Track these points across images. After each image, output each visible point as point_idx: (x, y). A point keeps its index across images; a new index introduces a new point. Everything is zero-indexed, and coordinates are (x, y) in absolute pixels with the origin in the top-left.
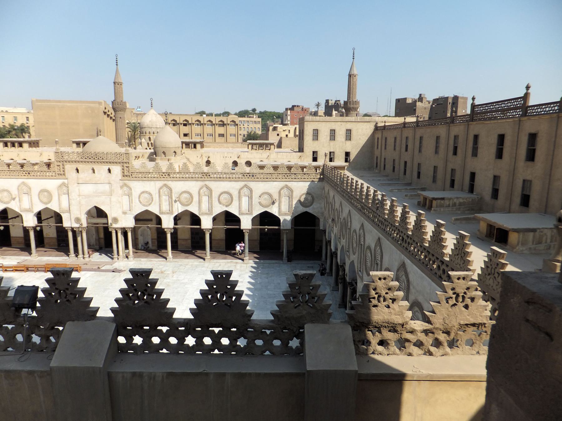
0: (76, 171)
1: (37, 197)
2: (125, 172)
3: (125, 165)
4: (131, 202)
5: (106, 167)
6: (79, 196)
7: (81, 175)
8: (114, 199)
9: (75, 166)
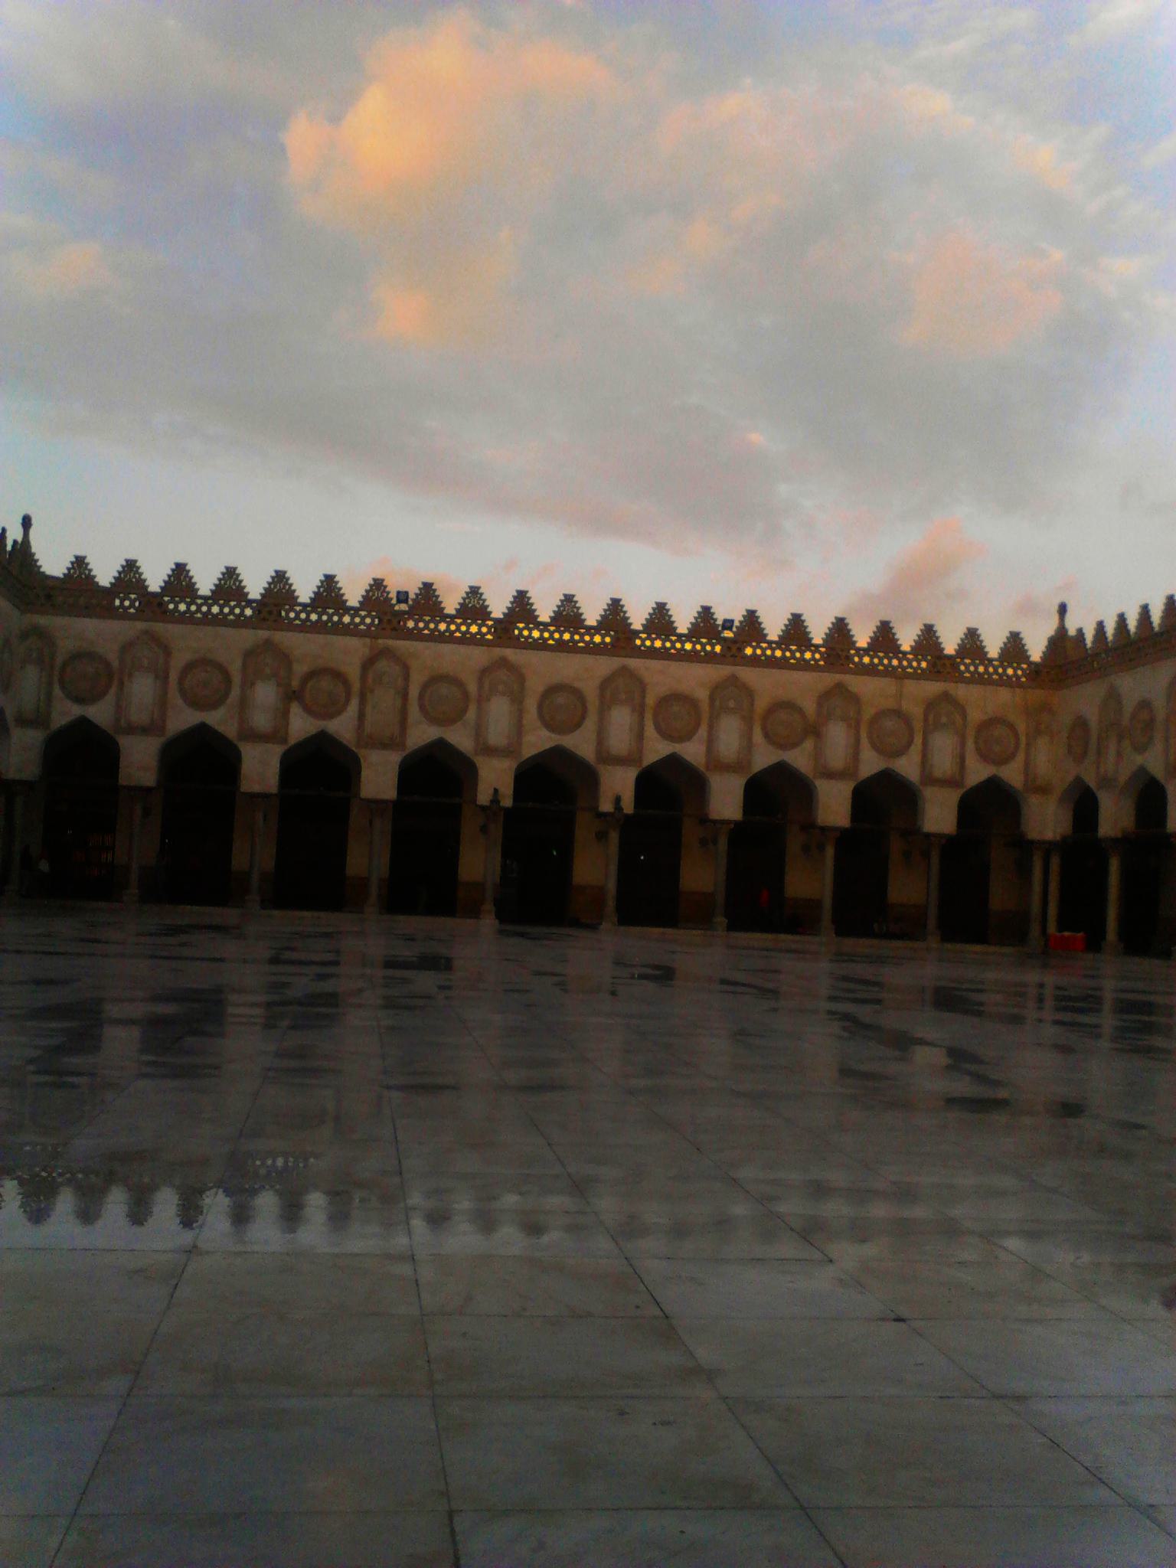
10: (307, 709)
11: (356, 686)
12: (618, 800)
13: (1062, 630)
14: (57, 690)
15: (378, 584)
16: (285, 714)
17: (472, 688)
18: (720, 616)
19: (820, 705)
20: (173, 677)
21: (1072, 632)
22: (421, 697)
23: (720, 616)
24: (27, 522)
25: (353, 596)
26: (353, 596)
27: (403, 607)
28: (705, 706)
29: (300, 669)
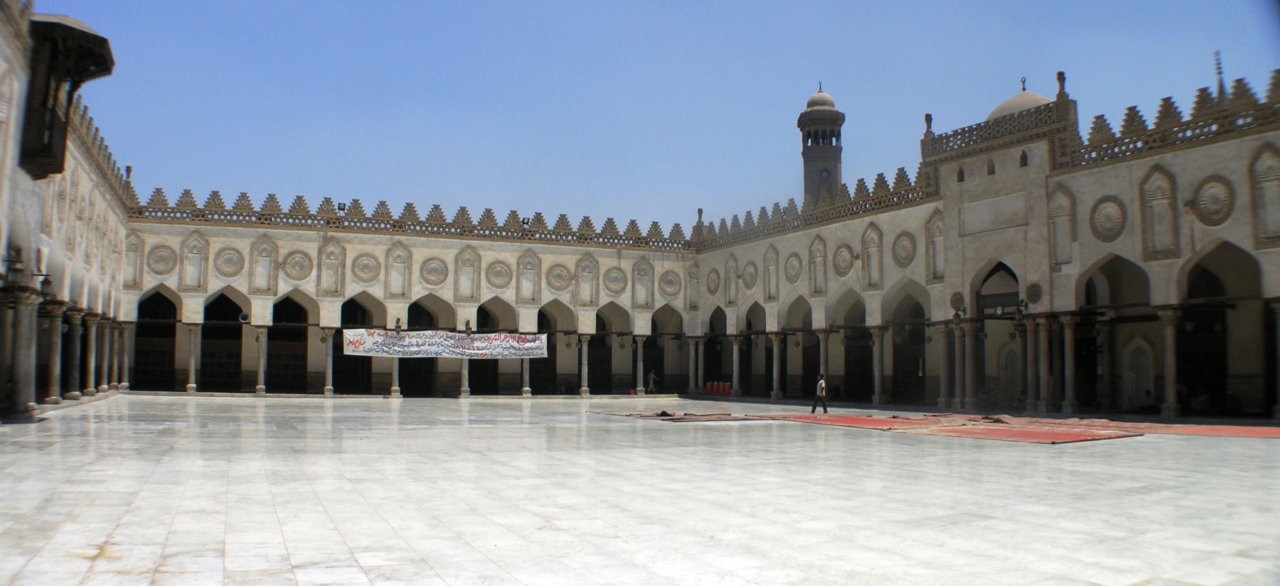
0: (955, 177)
2: (1058, 153)
3: (1057, 136)
5: (1016, 152)
7: (969, 184)
8: (1032, 234)
9: (955, 165)
10: (287, 274)
11: (315, 262)
12: (468, 323)
13: (700, 223)
14: (145, 267)
15: (328, 201)
16: (276, 278)
17: (382, 260)
18: (521, 217)
19: (577, 266)
20: (212, 257)
21: (706, 223)
22: (353, 265)
23: (521, 217)
24: (128, 169)
25: (313, 208)
26: (313, 208)
27: (342, 213)
28: (514, 267)
29: (283, 252)
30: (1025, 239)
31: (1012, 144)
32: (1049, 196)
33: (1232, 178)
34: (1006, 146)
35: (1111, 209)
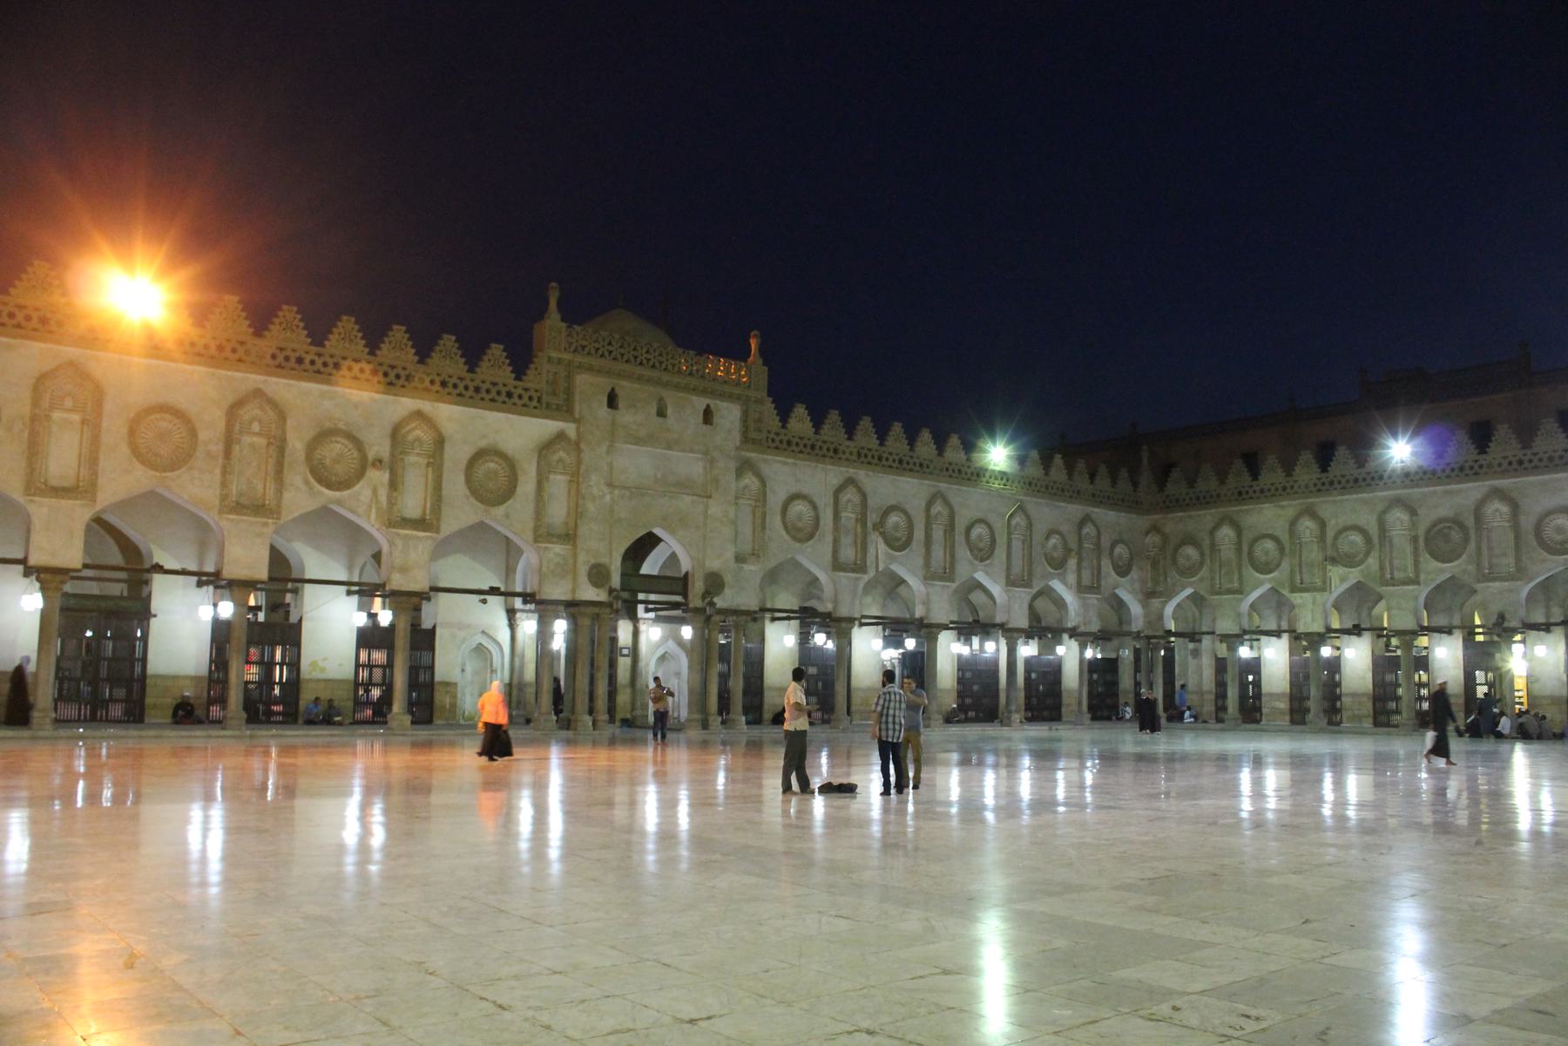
1: (461, 479)
4: (761, 525)
5: (701, 403)
6: (610, 485)
7: (626, 416)
8: (715, 509)
30: (706, 517)
31: (704, 392)
32: (739, 473)
33: (912, 512)
34: (695, 391)
35: (799, 507)
